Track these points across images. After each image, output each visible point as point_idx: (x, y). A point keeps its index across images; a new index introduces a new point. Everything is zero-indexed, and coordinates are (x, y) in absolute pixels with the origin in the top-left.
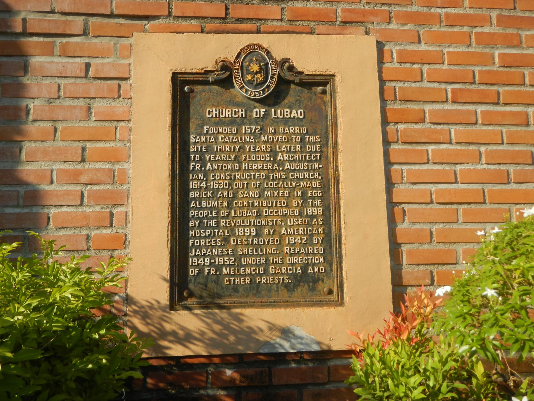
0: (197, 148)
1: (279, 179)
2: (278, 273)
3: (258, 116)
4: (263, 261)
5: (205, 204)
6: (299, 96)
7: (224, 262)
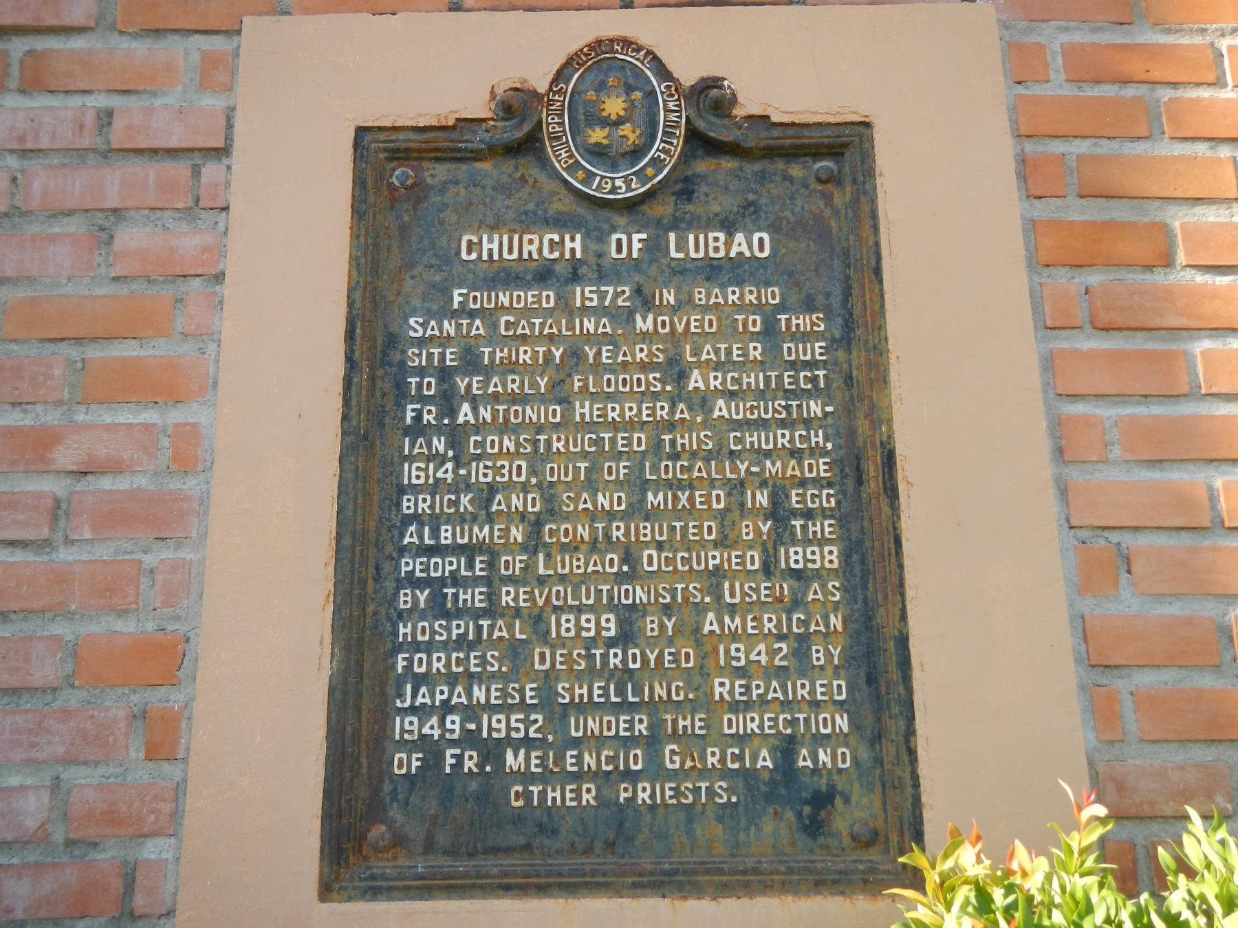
0: (430, 355)
1: (694, 455)
2: (693, 768)
3: (624, 255)
4: (641, 728)
5: (449, 534)
6: (755, 192)
7: (509, 728)
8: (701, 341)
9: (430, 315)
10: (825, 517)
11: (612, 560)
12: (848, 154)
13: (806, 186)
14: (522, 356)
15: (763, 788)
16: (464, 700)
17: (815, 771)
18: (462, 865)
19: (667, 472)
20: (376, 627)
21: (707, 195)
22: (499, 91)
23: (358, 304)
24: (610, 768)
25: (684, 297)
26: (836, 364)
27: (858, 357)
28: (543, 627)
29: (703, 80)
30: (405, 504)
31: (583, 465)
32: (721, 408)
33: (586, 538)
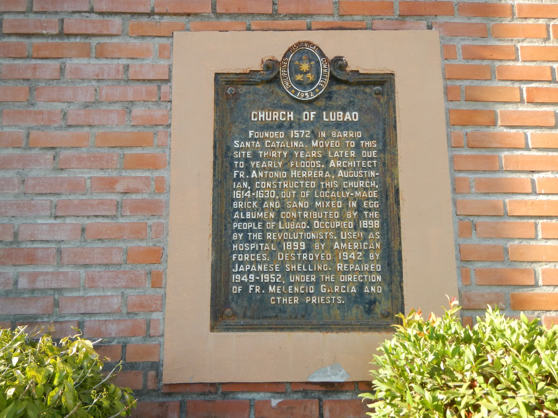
0: (242, 154)
1: (331, 189)
2: (330, 292)
3: (308, 120)
4: (313, 279)
5: (249, 215)
6: (353, 97)
7: (270, 279)
8: (334, 150)
9: (241, 140)
10: (375, 211)
11: (304, 224)
12: (386, 85)
13: (371, 96)
14: (273, 155)
15: (353, 299)
16: (255, 270)
17: (370, 294)
18: (256, 322)
19: (322, 195)
20: (225, 245)
21: (336, 98)
22: (265, 61)
23: (217, 136)
24: (303, 292)
25: (328, 134)
26: (380, 158)
27: (388, 156)
28: (281, 246)
29: (336, 57)
30: (234, 205)
31: (294, 192)
32: (341, 173)
33: (295, 217)
